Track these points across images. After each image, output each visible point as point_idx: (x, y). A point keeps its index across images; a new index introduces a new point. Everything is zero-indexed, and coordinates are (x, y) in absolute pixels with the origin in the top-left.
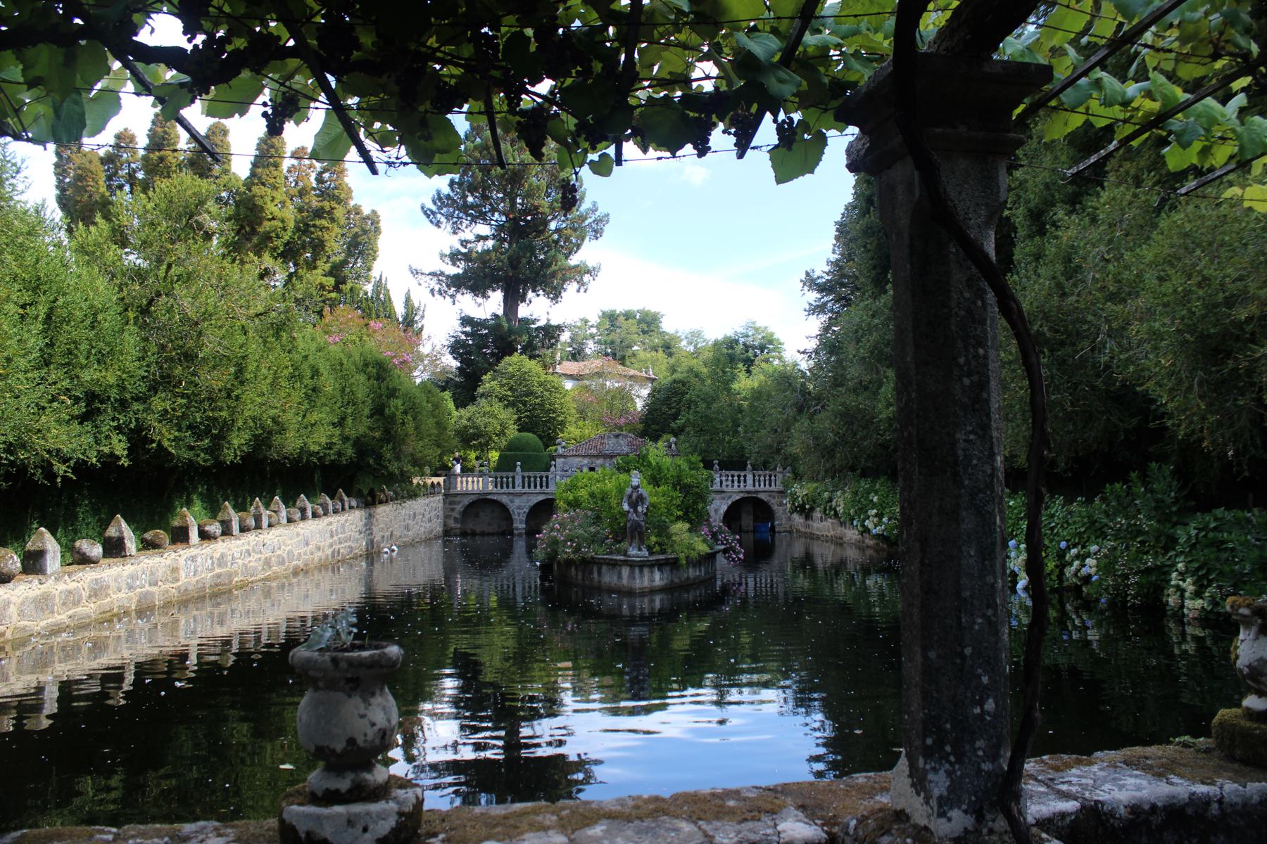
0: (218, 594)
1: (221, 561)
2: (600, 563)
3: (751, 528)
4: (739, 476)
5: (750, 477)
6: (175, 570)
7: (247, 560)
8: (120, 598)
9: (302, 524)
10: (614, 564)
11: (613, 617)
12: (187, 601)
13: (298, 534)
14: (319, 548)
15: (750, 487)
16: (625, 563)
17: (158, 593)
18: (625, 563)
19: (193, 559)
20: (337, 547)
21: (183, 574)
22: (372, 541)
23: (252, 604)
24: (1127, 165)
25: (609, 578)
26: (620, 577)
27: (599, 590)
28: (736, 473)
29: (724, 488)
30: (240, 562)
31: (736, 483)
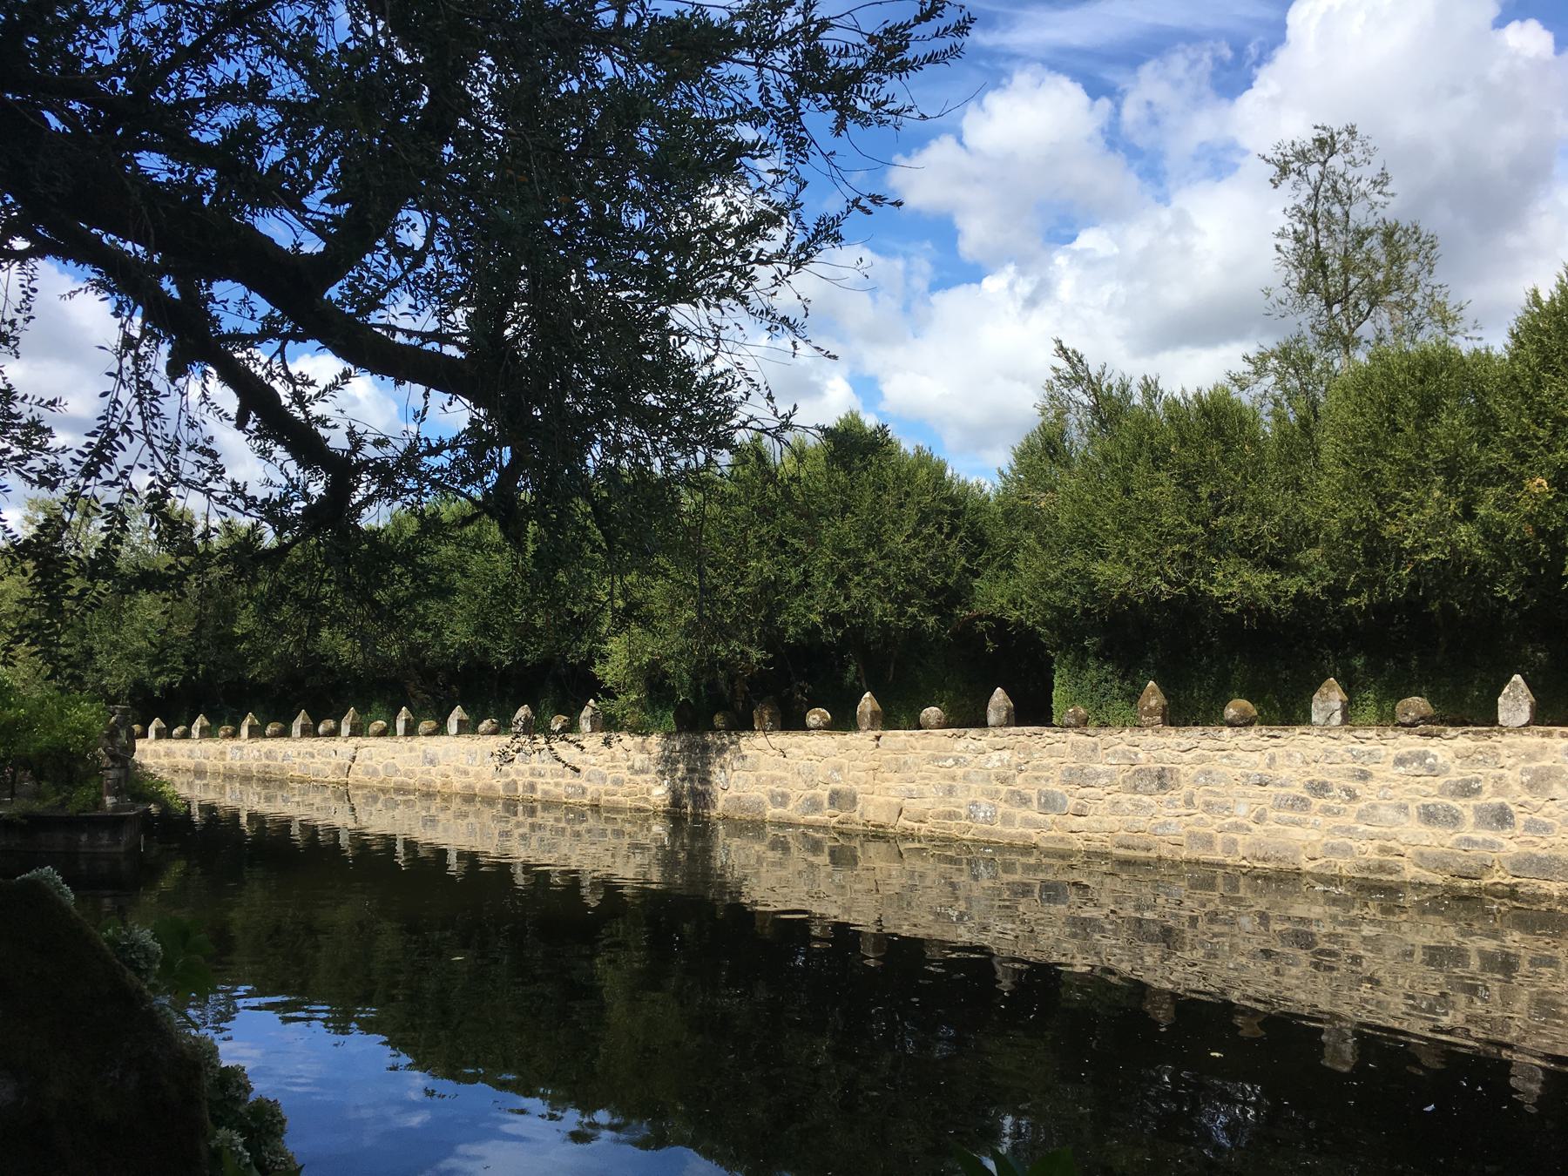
0: (269, 781)
1: (269, 755)
6: (223, 753)
7: (308, 761)
8: (182, 761)
9: (423, 739)
12: (229, 776)
13: (411, 750)
14: (466, 773)
17: (209, 765)
19: (240, 748)
20: (522, 782)
21: (228, 758)
22: (702, 798)
23: (317, 800)
30: (298, 760)
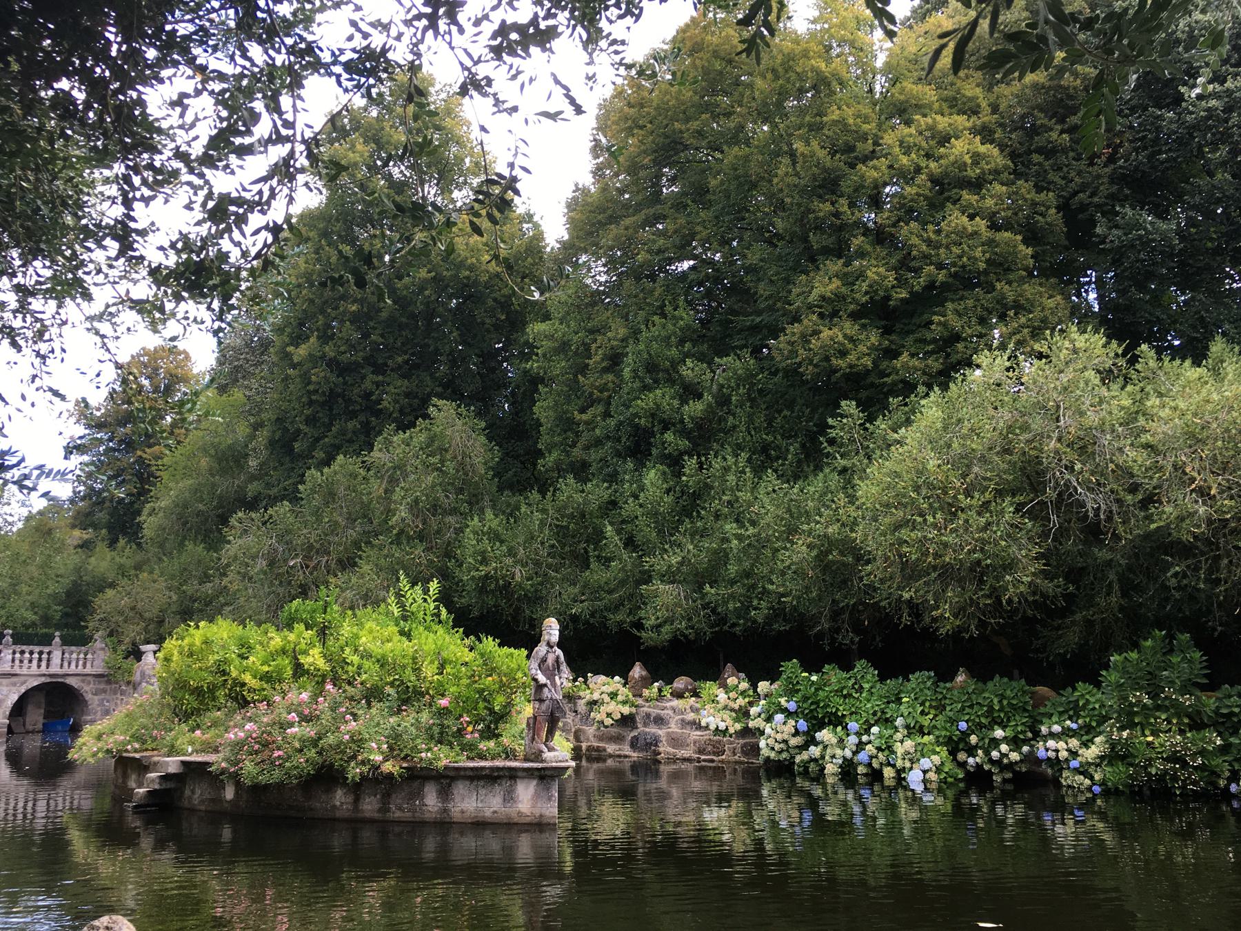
2: (447, 779)
3: (40, 726)
4: (41, 653)
5: (57, 655)
10: (491, 778)
11: (499, 872)
15: (55, 669)
16: (530, 773)
18: (530, 773)
24: (826, 333)
25: (470, 803)
26: (509, 797)
27: (444, 825)
28: (37, 649)
29: (17, 670)
31: (35, 662)
